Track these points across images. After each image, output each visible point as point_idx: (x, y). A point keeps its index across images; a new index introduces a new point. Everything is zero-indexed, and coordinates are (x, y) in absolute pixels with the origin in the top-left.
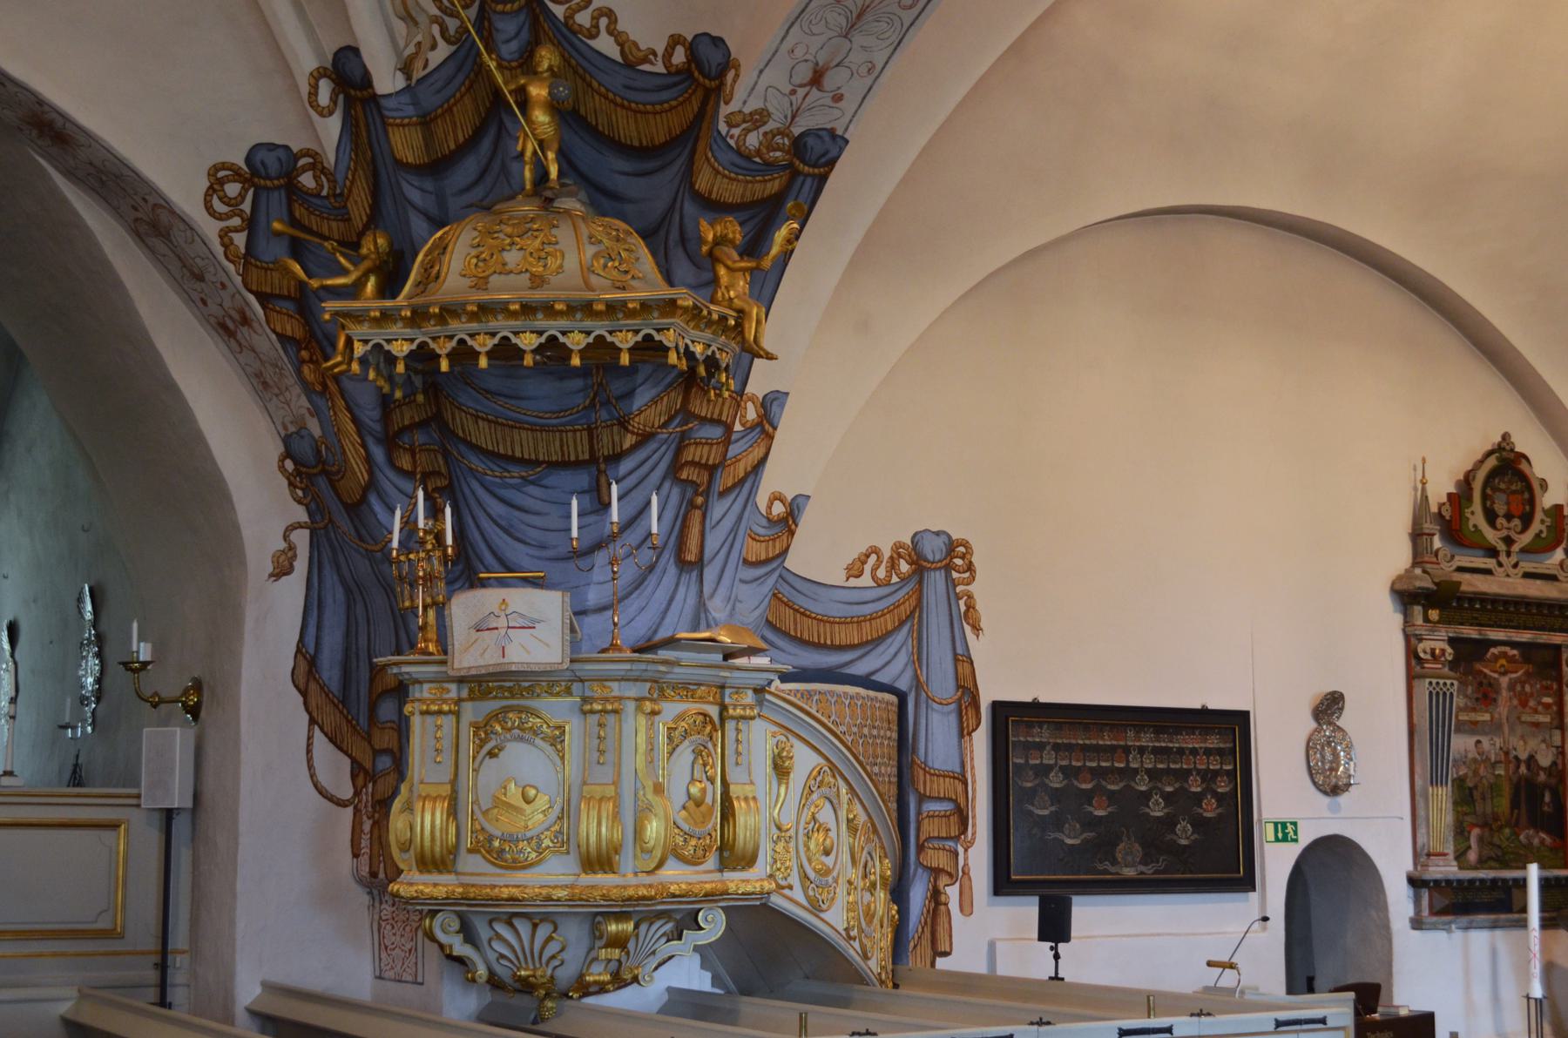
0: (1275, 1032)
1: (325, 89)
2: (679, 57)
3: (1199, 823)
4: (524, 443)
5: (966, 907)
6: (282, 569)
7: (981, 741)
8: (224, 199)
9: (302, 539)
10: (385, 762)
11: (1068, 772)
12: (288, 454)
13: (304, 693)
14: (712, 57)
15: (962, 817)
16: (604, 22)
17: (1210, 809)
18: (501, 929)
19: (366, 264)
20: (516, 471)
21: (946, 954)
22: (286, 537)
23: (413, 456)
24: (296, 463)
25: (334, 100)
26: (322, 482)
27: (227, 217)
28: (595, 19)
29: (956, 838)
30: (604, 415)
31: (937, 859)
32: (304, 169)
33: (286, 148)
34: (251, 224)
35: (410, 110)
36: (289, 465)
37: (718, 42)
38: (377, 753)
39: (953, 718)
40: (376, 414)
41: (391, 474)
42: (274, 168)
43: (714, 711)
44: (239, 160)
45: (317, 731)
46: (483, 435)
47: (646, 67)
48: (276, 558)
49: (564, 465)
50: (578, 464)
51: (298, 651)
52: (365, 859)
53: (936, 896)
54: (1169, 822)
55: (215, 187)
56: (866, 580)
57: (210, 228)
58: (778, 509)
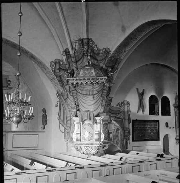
0: (172, 159)
1: (64, 53)
2: (104, 50)
3: (153, 133)
4: (85, 93)
5: (130, 144)
6: (57, 106)
7: (131, 124)
8: (52, 65)
9: (59, 103)
10: (69, 128)
11: (140, 128)
12: (57, 93)
13: (59, 120)
14: (108, 50)
15: (129, 133)
16: (96, 46)
17: (155, 131)
18: (85, 148)
19: (69, 73)
20: (84, 96)
21: (128, 148)
22: (57, 102)
24: (58, 94)
25: (65, 54)
26: (62, 97)
27: (53, 67)
28: (95, 46)
29: (128, 135)
30: (94, 90)
31: (126, 137)
32: (61, 62)
33: (59, 59)
34: (55, 68)
35: (74, 56)
36: (57, 94)
37: (109, 49)
38: (67, 127)
39: (128, 122)
40: (68, 89)
41: (70, 96)
42: (58, 62)
43: (107, 123)
44: (54, 61)
45: (60, 125)
46: (81, 92)
48: (56, 105)
49: (90, 95)
51: (58, 115)
52: (66, 139)
53: (126, 142)
54: (151, 133)
55: (51, 64)
56: (119, 106)
57: (50, 68)
58: (110, 99)
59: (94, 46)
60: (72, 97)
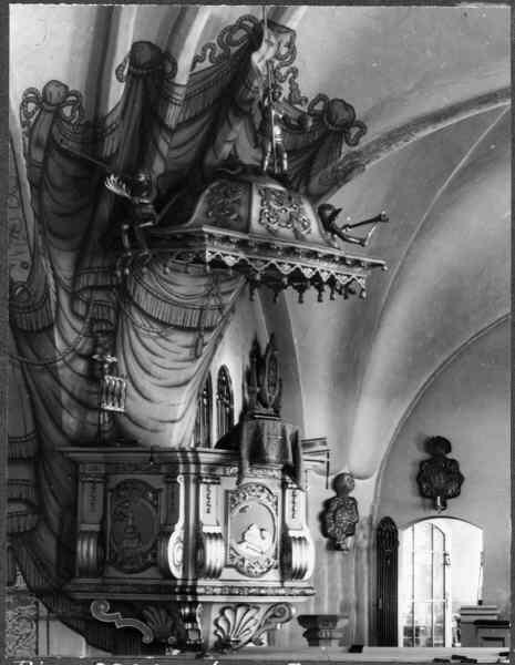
2: (319, 107)
14: (343, 115)
23: (88, 306)
33: (66, 87)
37: (348, 107)
47: (298, 106)
50: (189, 330)
59: (283, 71)
60: (79, 326)
